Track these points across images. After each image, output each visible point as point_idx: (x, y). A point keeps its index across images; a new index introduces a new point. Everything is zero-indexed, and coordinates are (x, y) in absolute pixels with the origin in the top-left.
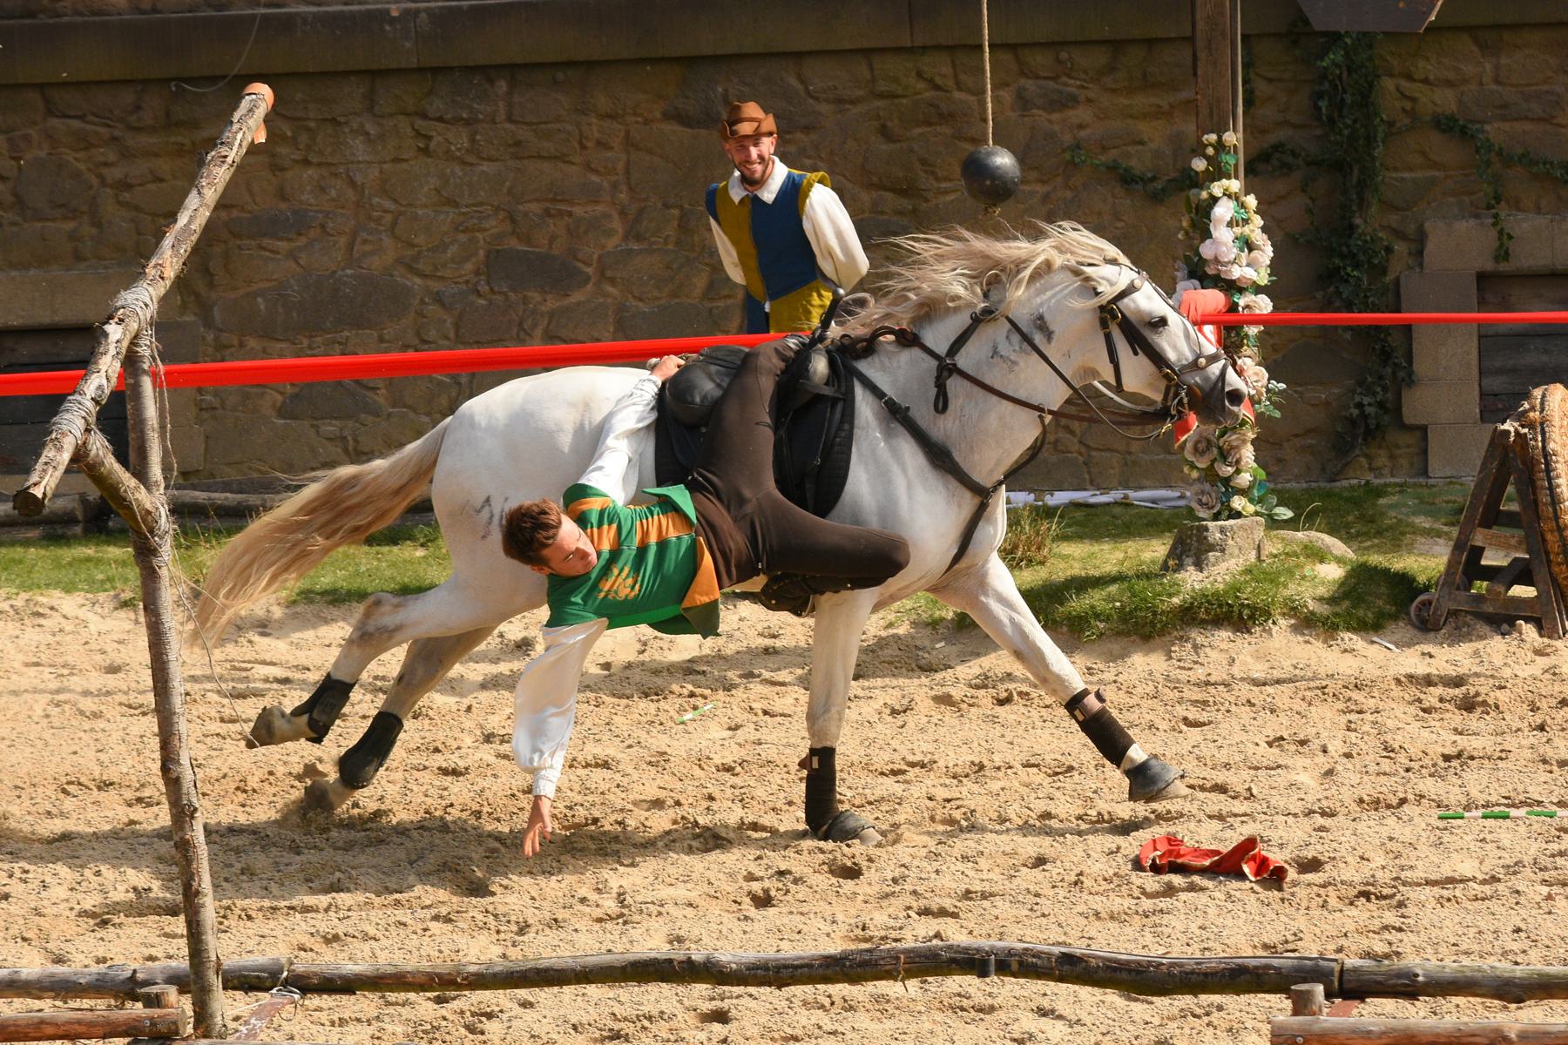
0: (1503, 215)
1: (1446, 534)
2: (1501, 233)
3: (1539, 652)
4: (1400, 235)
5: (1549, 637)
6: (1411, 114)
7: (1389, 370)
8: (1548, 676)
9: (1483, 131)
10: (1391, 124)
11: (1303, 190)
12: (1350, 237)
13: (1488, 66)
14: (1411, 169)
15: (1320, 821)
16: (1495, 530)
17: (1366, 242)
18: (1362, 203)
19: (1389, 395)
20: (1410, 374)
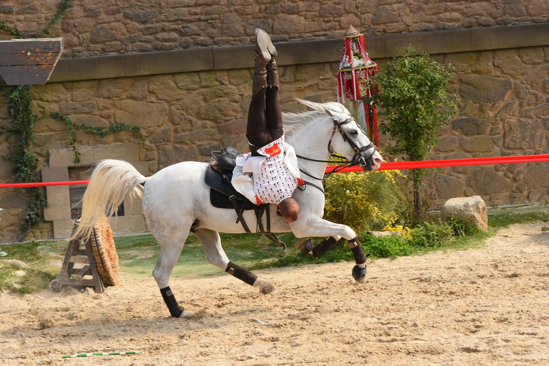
0: (76, 146)
1: (61, 258)
2: (76, 153)
3: (95, 298)
4: (40, 155)
5: (98, 293)
6: (43, 113)
7: (39, 202)
8: (98, 306)
9: (68, 118)
10: (36, 116)
11: (6, 141)
12: (23, 156)
13: (69, 95)
14: (43, 132)
15: (21, 360)
16: (78, 256)
17: (29, 158)
18: (27, 144)
19: (39, 211)
20: (46, 203)
